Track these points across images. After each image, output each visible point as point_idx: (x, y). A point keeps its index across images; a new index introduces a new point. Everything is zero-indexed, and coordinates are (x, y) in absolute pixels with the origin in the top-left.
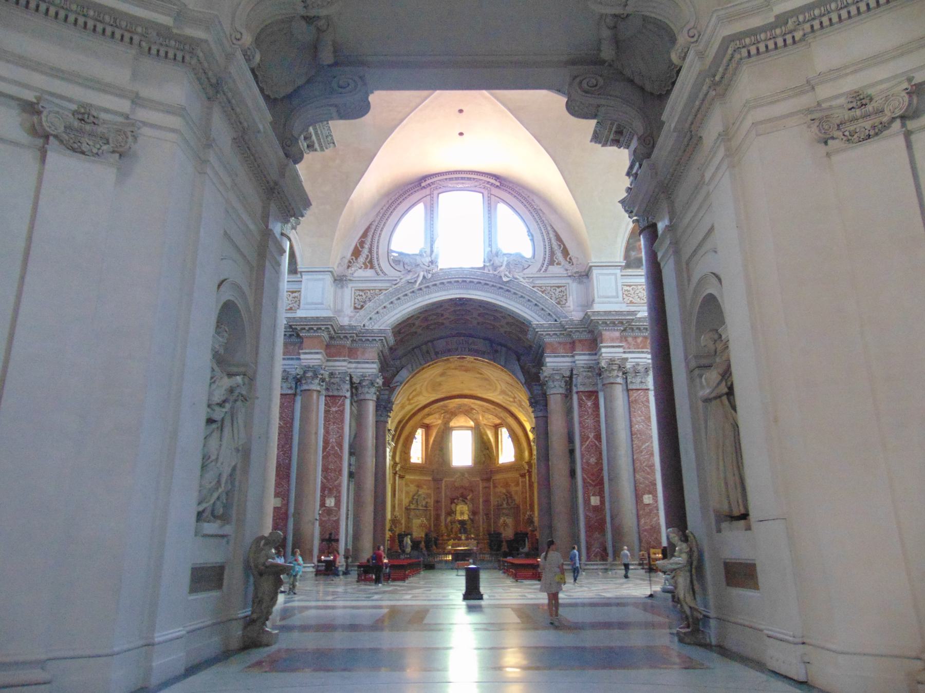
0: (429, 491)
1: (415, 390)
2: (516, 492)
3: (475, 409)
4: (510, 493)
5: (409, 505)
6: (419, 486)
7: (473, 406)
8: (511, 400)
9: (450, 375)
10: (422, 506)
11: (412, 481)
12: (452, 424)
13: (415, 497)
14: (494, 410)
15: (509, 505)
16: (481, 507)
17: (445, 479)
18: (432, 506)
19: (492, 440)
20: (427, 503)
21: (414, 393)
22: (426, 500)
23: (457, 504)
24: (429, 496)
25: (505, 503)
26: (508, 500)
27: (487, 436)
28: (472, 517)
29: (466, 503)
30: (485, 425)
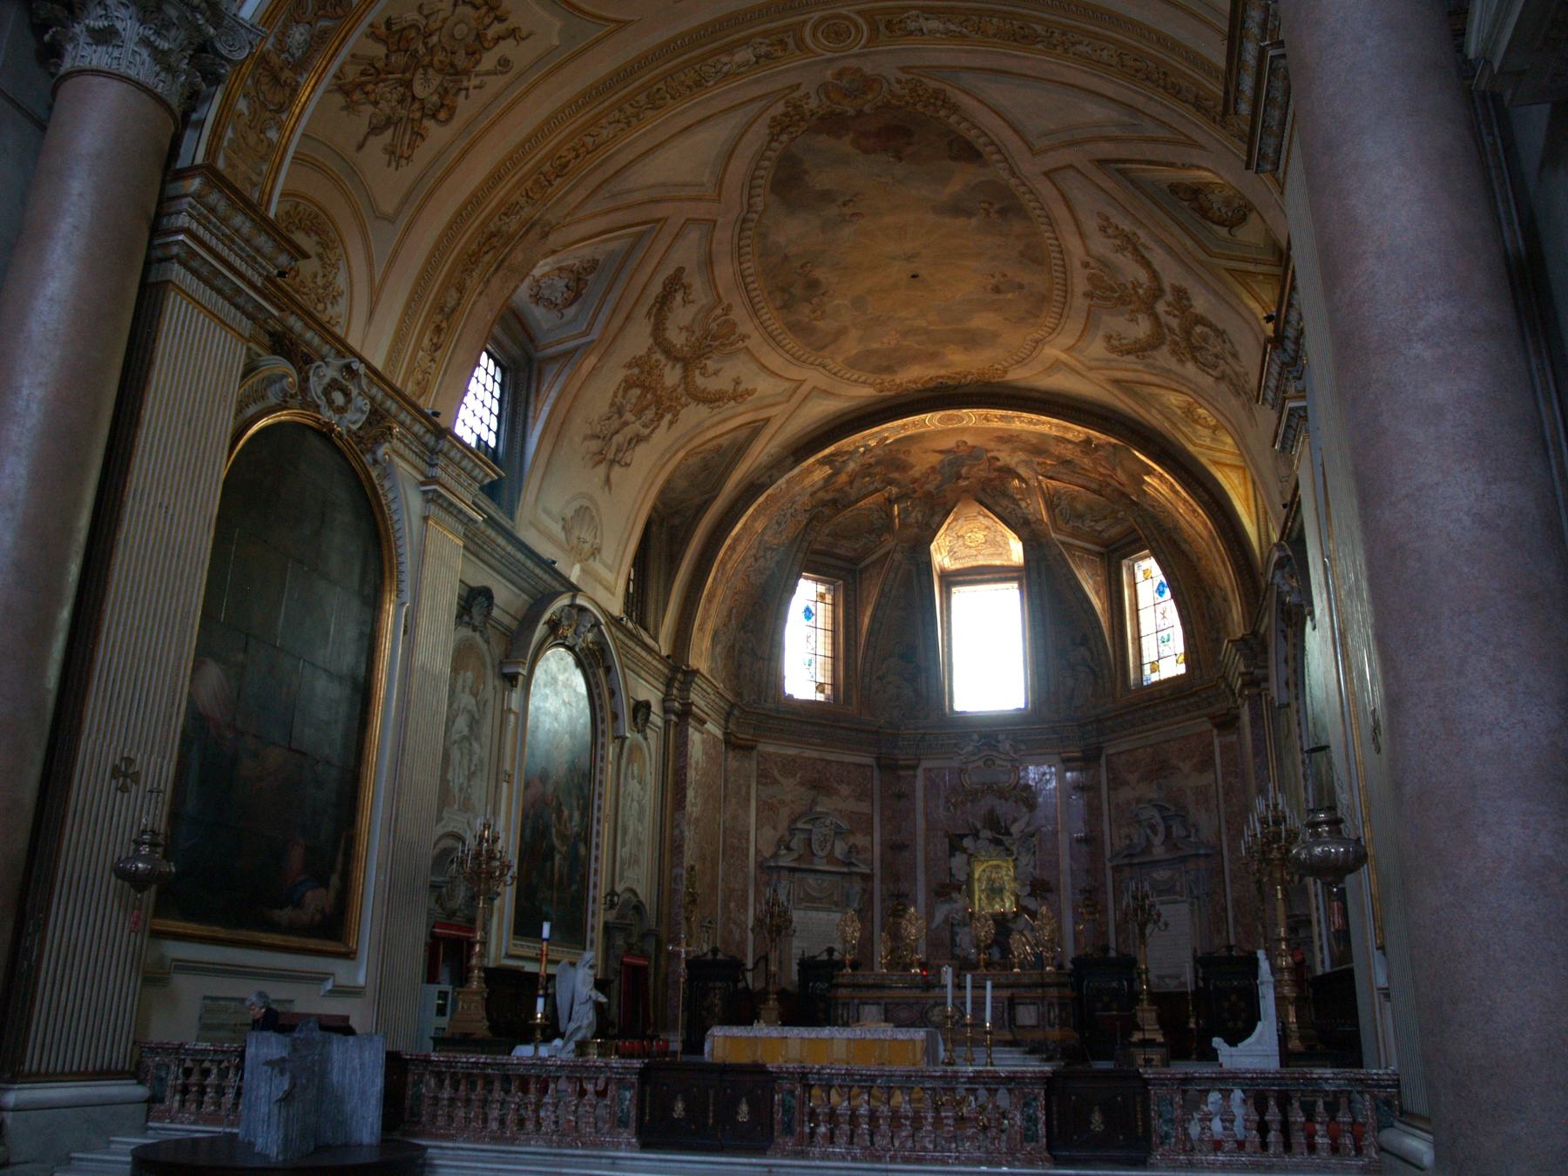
0: (863, 807)
1: (675, 283)
5: (775, 856)
6: (819, 785)
7: (1006, 457)
8: (1142, 329)
9: (826, 196)
10: (831, 858)
12: (942, 555)
13: (800, 825)
14: (1087, 462)
16: (1065, 862)
17: (925, 764)
18: (877, 864)
20: (852, 849)
21: (681, 316)
22: (852, 840)
24: (863, 823)
25: (1158, 840)
26: (1168, 829)
28: (1031, 904)
29: (1009, 852)
30: (1063, 543)
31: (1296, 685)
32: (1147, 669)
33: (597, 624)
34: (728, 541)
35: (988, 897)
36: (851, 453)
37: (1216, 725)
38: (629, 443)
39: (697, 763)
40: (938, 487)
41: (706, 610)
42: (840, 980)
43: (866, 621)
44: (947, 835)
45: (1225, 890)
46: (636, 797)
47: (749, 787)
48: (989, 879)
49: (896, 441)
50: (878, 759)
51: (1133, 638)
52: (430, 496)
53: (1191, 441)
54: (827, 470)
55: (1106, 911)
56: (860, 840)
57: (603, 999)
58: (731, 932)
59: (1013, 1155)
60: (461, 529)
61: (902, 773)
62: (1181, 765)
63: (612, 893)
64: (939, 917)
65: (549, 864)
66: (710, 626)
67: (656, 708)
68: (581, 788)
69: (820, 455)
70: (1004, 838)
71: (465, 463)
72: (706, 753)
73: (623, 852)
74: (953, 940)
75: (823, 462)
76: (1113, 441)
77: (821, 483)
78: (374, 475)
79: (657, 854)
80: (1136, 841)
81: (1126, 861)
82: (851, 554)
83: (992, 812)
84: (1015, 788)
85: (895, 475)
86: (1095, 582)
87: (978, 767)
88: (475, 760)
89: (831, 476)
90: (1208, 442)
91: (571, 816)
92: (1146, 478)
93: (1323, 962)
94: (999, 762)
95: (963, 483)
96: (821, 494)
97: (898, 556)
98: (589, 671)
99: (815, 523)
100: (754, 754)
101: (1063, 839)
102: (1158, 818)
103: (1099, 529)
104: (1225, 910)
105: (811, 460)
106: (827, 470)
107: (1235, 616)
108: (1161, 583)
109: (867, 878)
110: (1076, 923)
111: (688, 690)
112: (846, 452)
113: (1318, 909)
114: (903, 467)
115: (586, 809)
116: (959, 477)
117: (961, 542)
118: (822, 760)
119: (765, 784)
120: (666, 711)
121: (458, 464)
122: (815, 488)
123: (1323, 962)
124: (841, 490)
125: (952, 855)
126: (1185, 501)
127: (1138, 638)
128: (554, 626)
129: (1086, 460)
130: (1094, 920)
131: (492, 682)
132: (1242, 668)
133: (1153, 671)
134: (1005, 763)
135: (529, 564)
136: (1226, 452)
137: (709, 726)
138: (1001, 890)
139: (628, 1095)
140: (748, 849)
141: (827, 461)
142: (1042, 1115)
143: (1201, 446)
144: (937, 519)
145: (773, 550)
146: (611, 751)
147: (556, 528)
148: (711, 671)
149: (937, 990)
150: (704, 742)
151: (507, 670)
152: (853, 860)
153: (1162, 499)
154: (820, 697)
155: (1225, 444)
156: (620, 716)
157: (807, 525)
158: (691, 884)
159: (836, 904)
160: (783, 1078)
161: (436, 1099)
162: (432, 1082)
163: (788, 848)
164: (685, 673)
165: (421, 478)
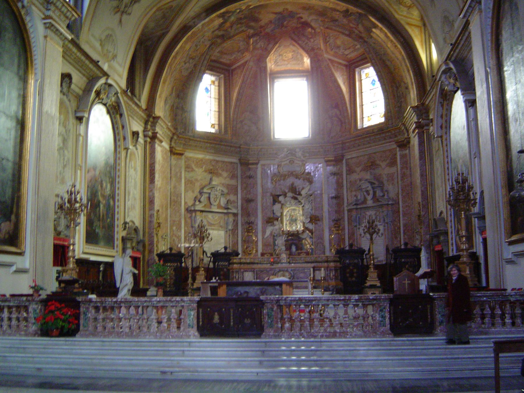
0: (233, 182)
2: (391, 177)
3: (312, 28)
4: (378, 178)
5: (194, 205)
7: (306, 17)
10: (219, 206)
11: (200, 163)
12: (271, 65)
13: (205, 190)
14: (345, 21)
15: (378, 201)
17: (262, 162)
18: (240, 208)
19: (344, 88)
23: (282, 204)
25: (369, 198)
26: (375, 193)
27: (336, 81)
28: (311, 226)
30: (330, 60)
31: (446, 127)
32: (365, 120)
33: (116, 93)
34: (173, 54)
35: (290, 223)
36: (233, 12)
37: (399, 146)
38: (131, 3)
39: (159, 161)
40: (272, 31)
41: (163, 87)
42: (235, 261)
43: (235, 94)
44: (271, 195)
45: (399, 220)
46: (133, 177)
47: (181, 173)
48: (290, 215)
49: (254, 7)
50: (240, 160)
51: (360, 106)
52: (48, 25)
53: (397, 12)
54: (221, 20)
55: (344, 229)
56: (232, 197)
57: (136, 272)
58: (174, 240)
59: (376, 333)
60: (61, 43)
61: (250, 166)
62: (381, 164)
63: (125, 223)
64: (268, 233)
65: (98, 209)
66: (164, 96)
67: (141, 135)
68: (110, 173)
69: (218, 13)
70: (298, 197)
71: (64, 9)
72: (162, 156)
73: (129, 204)
74: (274, 243)
75: (219, 16)
76: (360, 11)
77: (217, 27)
78: (23, 13)
79: (142, 205)
80: (359, 197)
81: (355, 207)
82: (228, 62)
83: (293, 184)
84: (303, 174)
85: (252, 24)
86: (343, 79)
87: (286, 164)
88: (66, 158)
89: (223, 23)
90: (405, 13)
91: (106, 186)
92: (374, 30)
93: (453, 250)
94: (296, 162)
95: (283, 29)
96: (216, 32)
97: (251, 64)
98: (113, 116)
99: (213, 46)
100: (183, 157)
101: (325, 198)
102: (370, 188)
103: (346, 52)
104: (399, 228)
105: (214, 15)
106: (221, 20)
107: (412, 96)
108: (374, 80)
109: (235, 215)
110: (330, 235)
111: (155, 127)
112: (230, 12)
113: (451, 227)
114: (257, 20)
115: (113, 183)
116: (282, 26)
117: (281, 57)
118: (214, 160)
119: (189, 171)
120: (145, 136)
121: (60, 10)
122: (215, 29)
123: (453, 250)
124: (226, 30)
125: (274, 204)
126: (392, 41)
127: (362, 105)
128: (98, 93)
129: (345, 20)
130: (339, 234)
131: (72, 121)
132: (416, 121)
133: (369, 121)
134: (298, 162)
135: (87, 62)
136: (414, 19)
137: (164, 144)
138: (296, 220)
139: (192, 313)
140: (181, 202)
141: (222, 15)
142: (387, 315)
143: (402, 15)
144: (271, 46)
145: (193, 59)
146: (123, 153)
147: (97, 45)
148: (164, 117)
149: (279, 264)
150: (162, 151)
151: (79, 115)
152: (230, 207)
153: (380, 40)
154: (213, 131)
155: (413, 15)
156: (127, 138)
157: (209, 47)
158: (158, 218)
159: (221, 227)
160: (268, 303)
161: (96, 319)
162: (93, 311)
163: (200, 201)
164: (154, 118)
165: (43, 16)
